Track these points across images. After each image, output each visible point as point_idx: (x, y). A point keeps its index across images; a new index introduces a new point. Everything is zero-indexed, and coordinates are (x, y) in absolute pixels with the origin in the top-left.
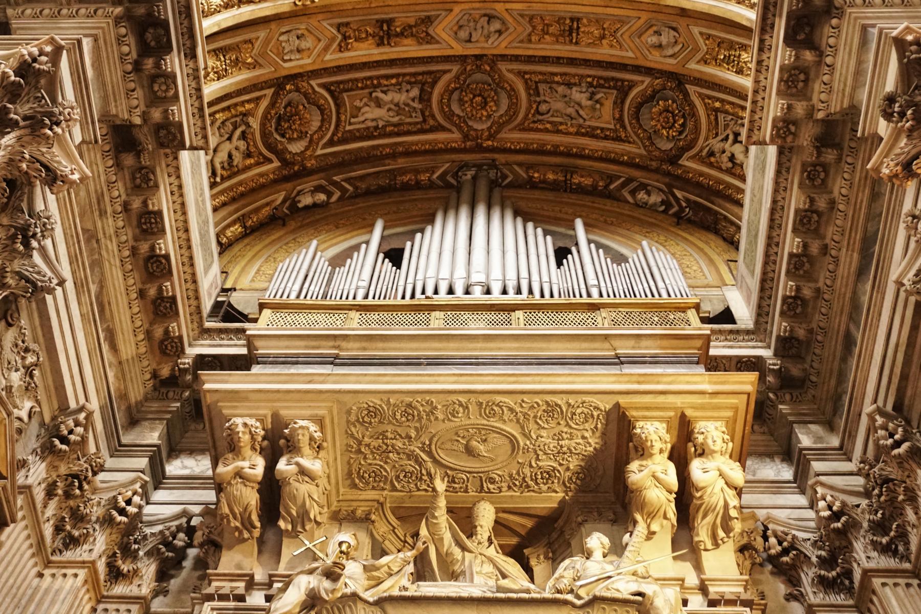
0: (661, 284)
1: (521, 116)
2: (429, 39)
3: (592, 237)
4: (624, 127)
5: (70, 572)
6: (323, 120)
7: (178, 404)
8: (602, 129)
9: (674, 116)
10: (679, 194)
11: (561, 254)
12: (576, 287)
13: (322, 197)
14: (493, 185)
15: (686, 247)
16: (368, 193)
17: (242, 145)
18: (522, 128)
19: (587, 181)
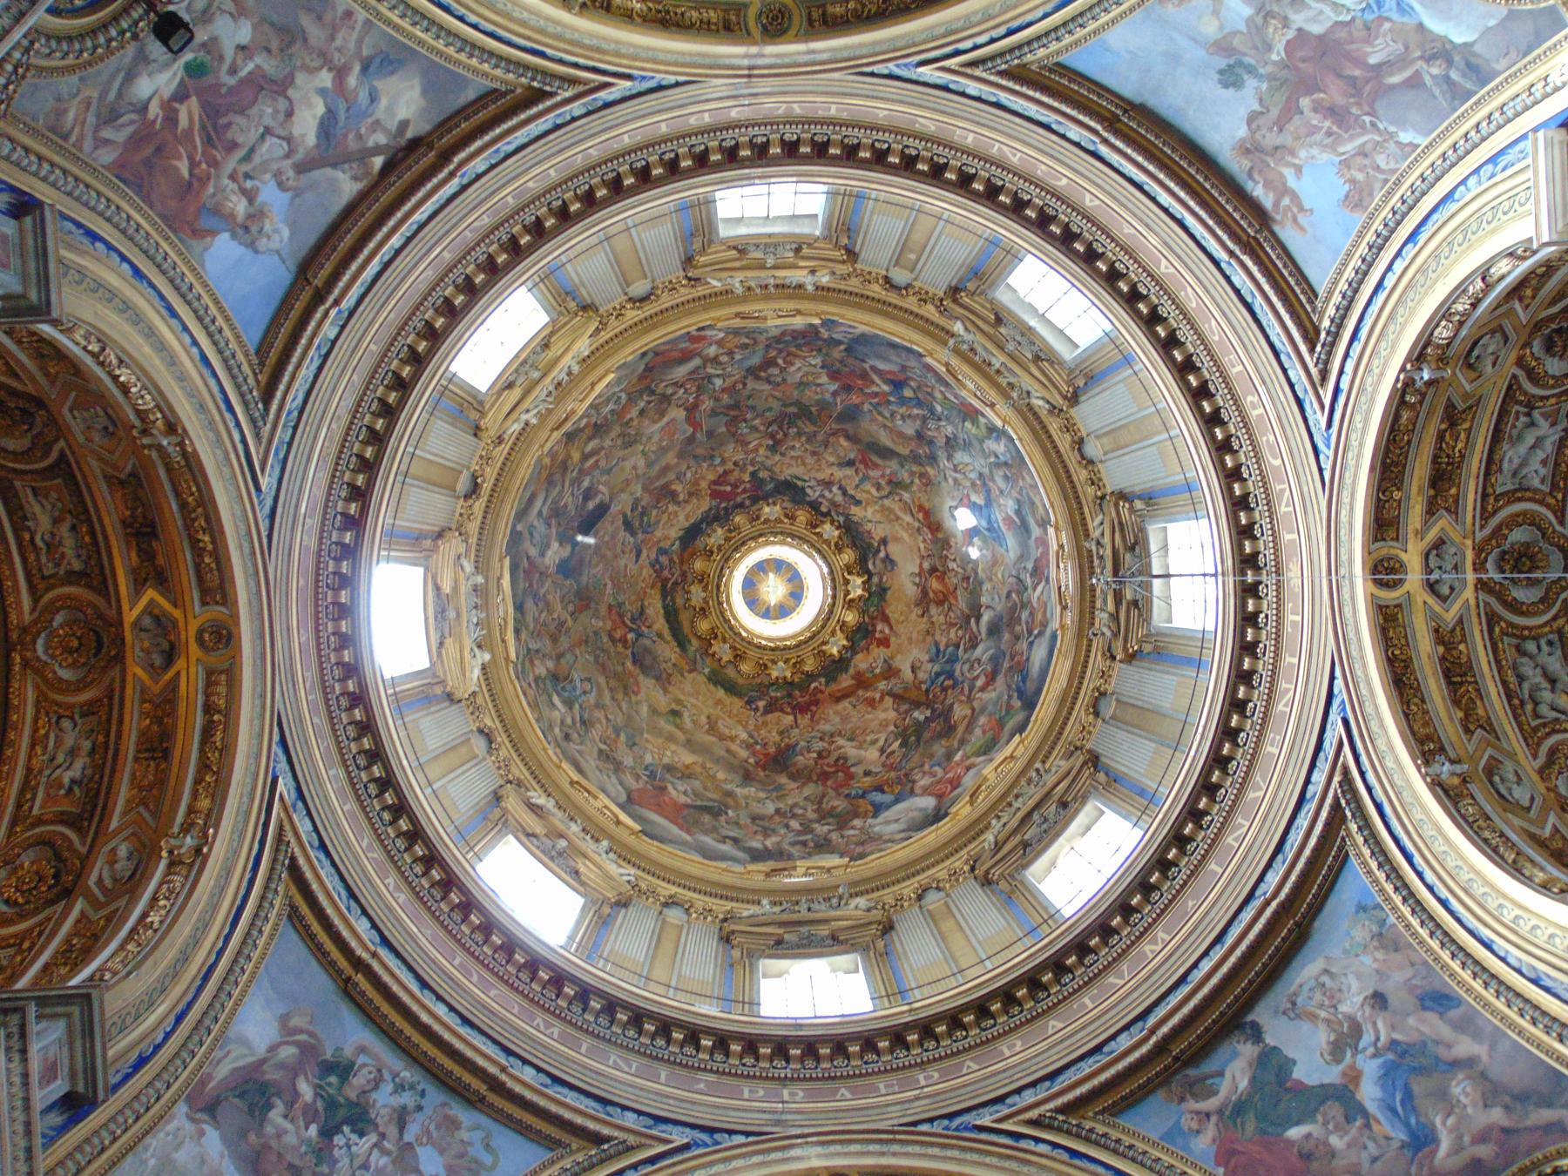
2: (139, 585)
6: (15, 453)
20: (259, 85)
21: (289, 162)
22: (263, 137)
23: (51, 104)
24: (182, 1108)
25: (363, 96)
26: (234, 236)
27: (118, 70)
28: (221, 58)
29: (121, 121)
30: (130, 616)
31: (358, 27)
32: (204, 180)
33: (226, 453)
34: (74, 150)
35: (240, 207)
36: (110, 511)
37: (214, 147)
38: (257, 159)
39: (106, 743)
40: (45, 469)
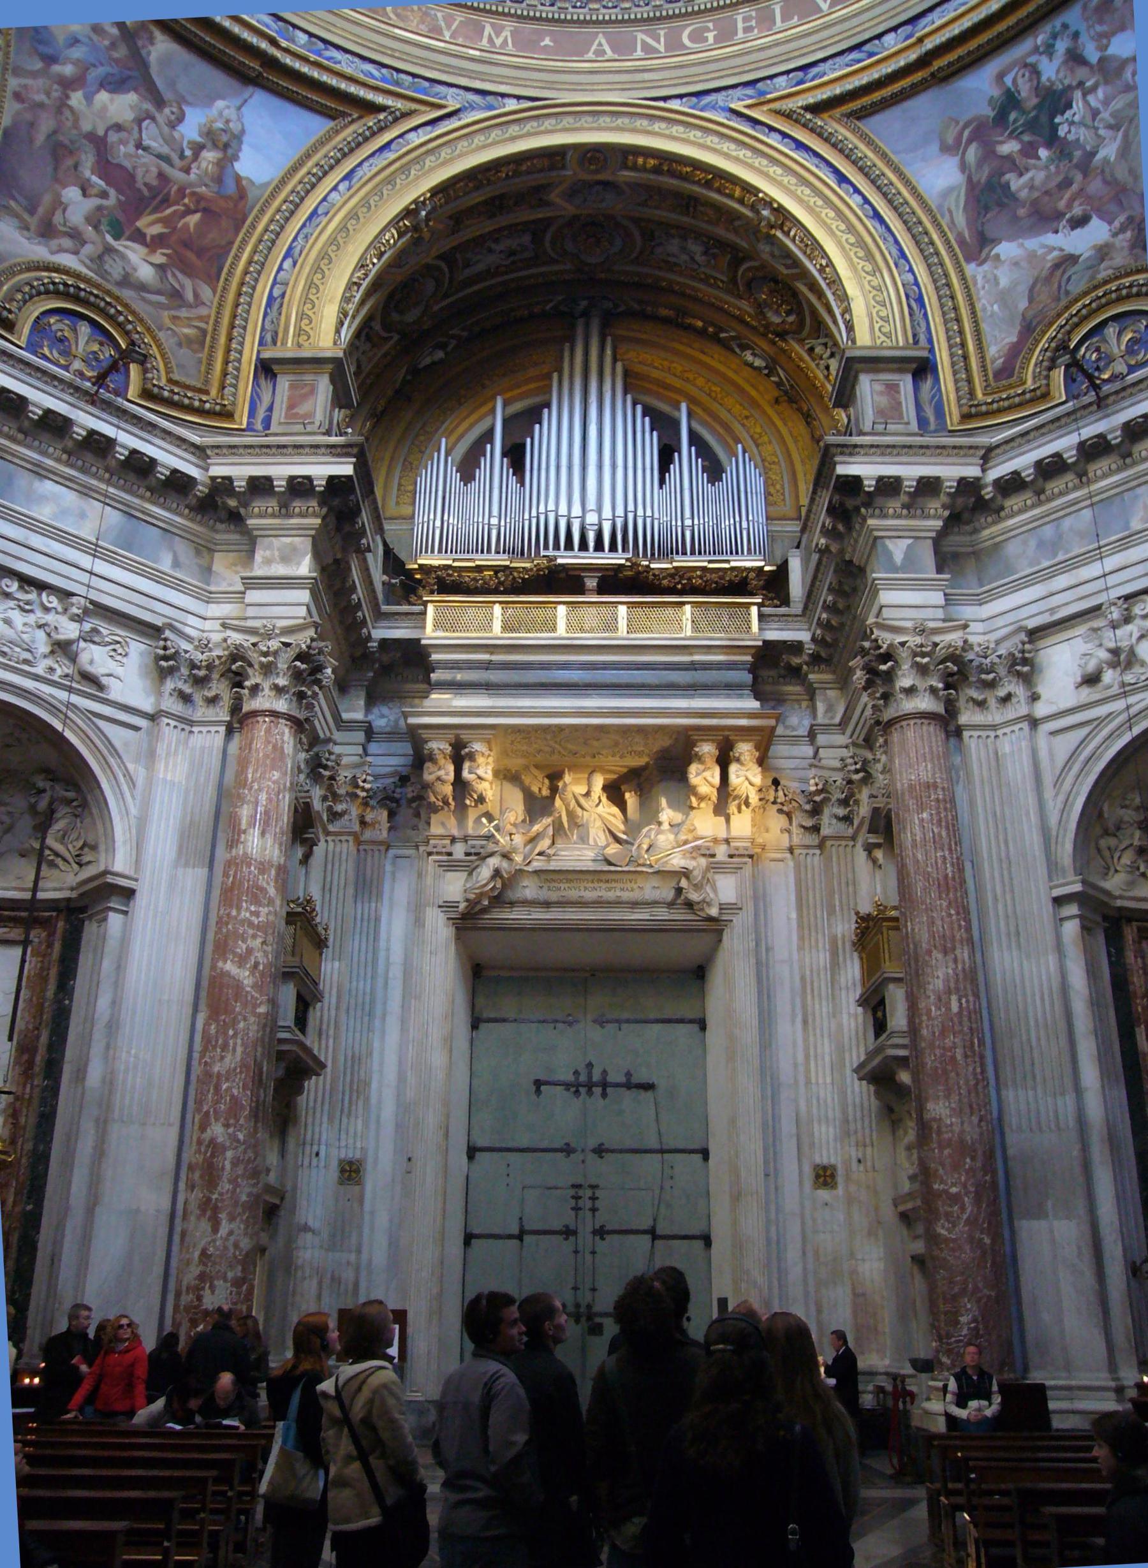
0: (744, 525)
5: (343, 838)
8: (715, 278)
13: (440, 355)
20: (107, 167)
21: (157, 115)
22: (145, 149)
23: (184, 351)
24: (970, 269)
25: (77, 53)
26: (236, 158)
27: (144, 299)
28: (99, 208)
29: (177, 286)
31: (24, 81)
32: (198, 198)
33: (428, 152)
34: (211, 322)
35: (210, 156)
37: (168, 194)
38: (165, 150)
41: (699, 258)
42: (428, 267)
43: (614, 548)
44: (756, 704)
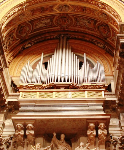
0: (100, 76)
1: (73, 24)
2: (53, 11)
3: (88, 58)
4: (95, 29)
6: (29, 29)
7: (6, 111)
8: (91, 28)
9: (106, 30)
10: (106, 46)
11: (81, 64)
12: (83, 76)
13: (30, 45)
14: (68, 39)
15: (107, 63)
16: (40, 42)
17: (12, 39)
18: (74, 26)
19: (88, 39)
30: (59, 12)
36: (38, 15)
39: (82, 17)
40: (32, 24)
41: (87, 24)
42: (25, 22)
43: (68, 81)
44: (105, 113)
